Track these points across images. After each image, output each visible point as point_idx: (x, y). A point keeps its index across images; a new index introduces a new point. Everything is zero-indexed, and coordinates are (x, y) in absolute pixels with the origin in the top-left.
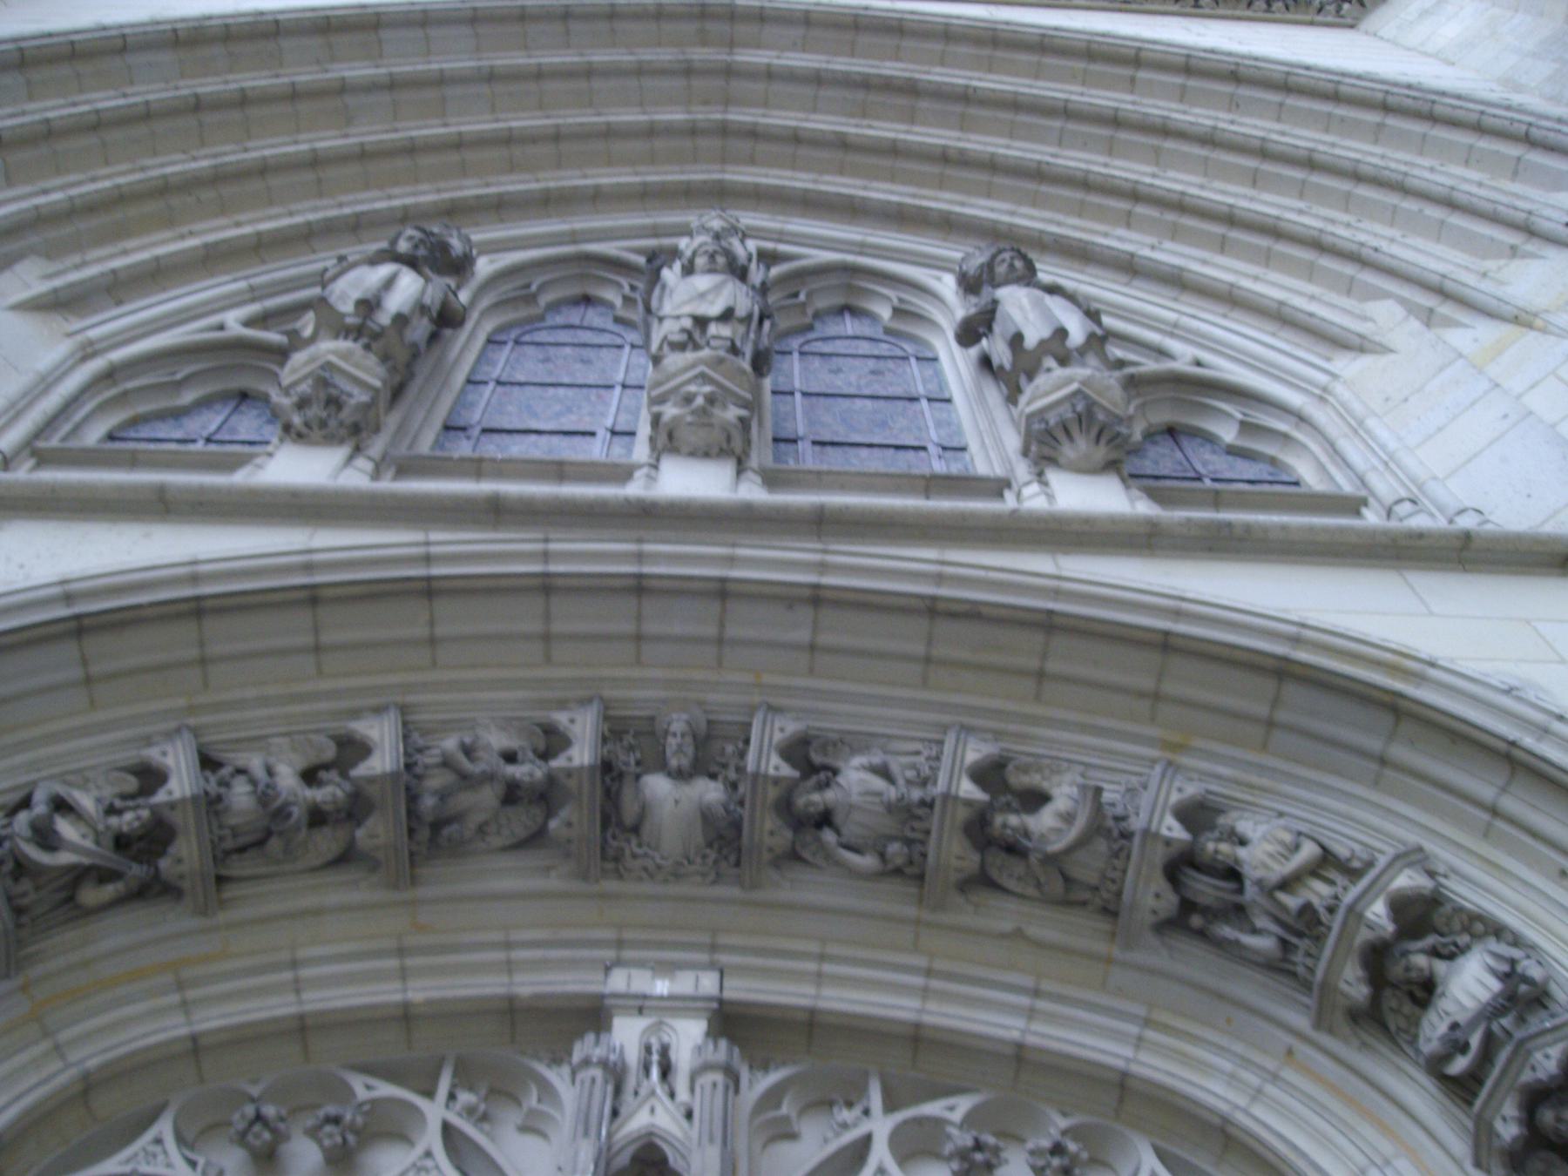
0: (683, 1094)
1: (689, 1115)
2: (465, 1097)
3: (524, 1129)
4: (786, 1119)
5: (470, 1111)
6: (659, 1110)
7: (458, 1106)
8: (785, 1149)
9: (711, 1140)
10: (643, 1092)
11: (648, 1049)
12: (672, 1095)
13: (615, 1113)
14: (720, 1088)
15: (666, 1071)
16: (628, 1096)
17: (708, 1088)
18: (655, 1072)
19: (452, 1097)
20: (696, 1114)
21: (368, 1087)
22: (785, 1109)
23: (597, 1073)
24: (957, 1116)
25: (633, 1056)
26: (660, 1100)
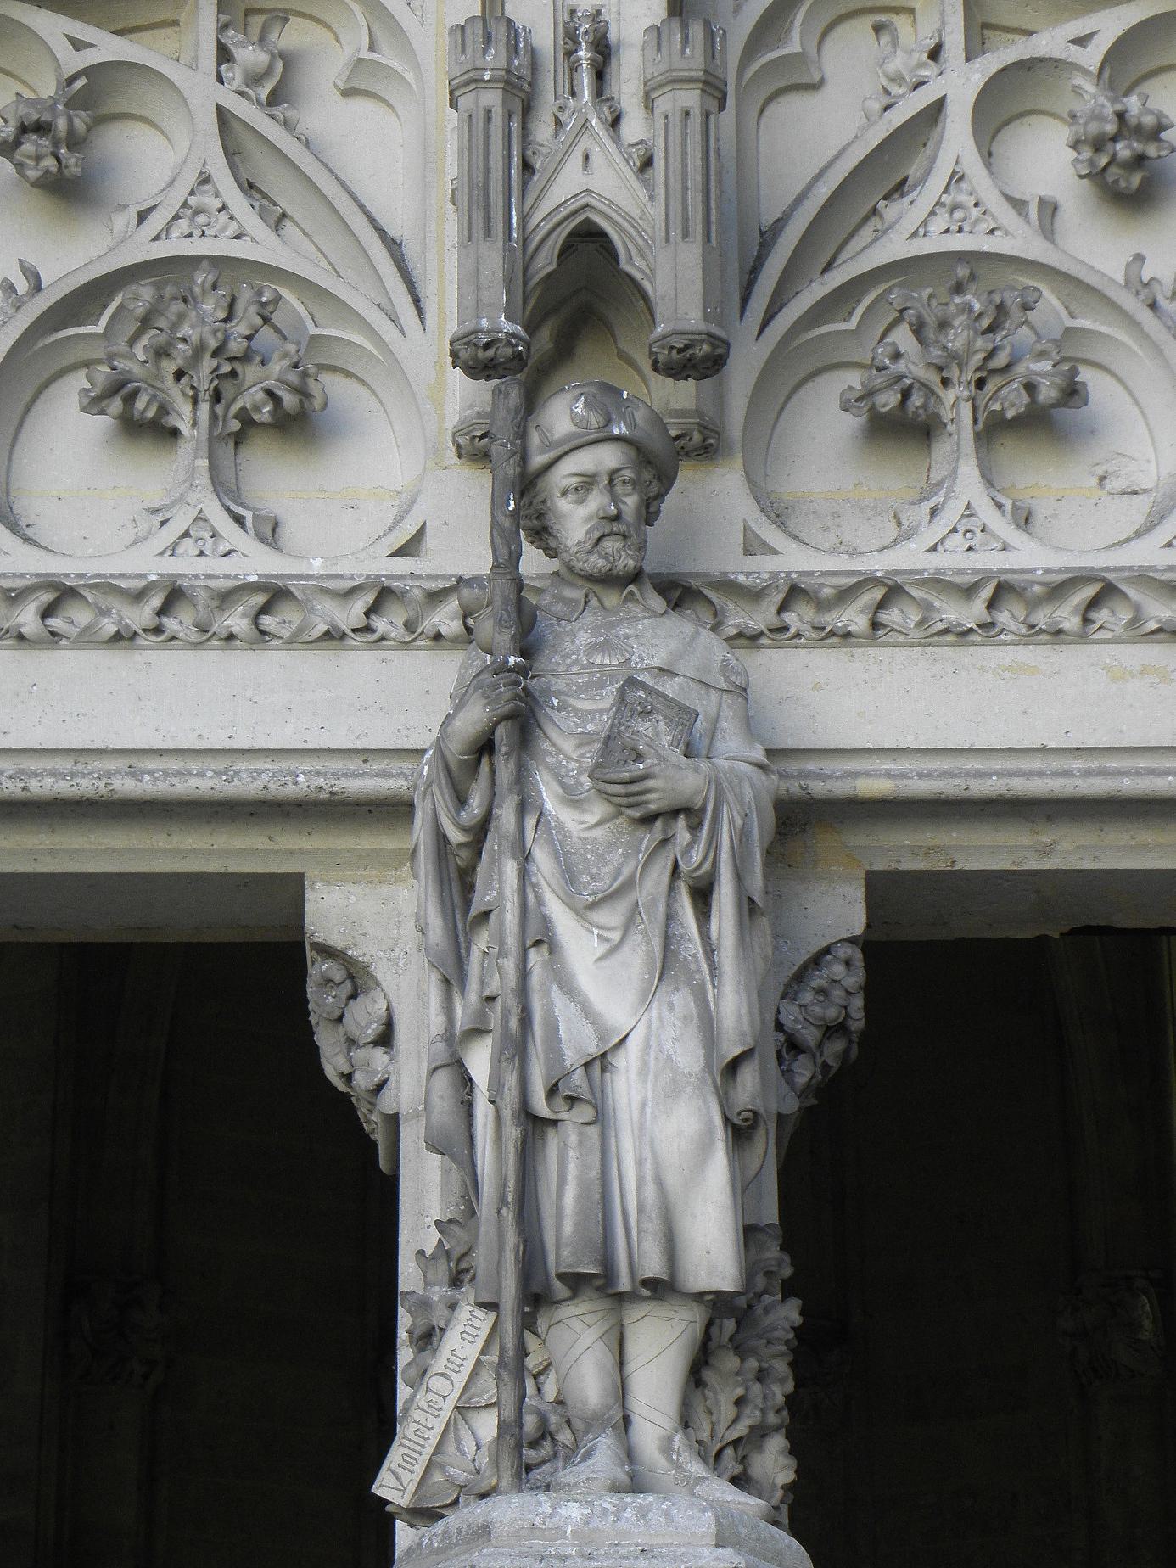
0: (634, 128)
1: (648, 163)
2: (249, 55)
3: (347, 93)
4: (799, 59)
5: (255, 79)
6: (597, 158)
7: (235, 74)
8: (794, 104)
9: (686, 235)
10: (571, 124)
11: (571, 35)
12: (615, 122)
13: (527, 167)
14: (696, 114)
15: (604, 51)
16: (543, 131)
17: (677, 118)
18: (586, 81)
19: (224, 55)
20: (659, 163)
21: (78, 45)
22: (794, 46)
23: (492, 98)
24: (1092, 56)
25: (545, 38)
26: (596, 138)
